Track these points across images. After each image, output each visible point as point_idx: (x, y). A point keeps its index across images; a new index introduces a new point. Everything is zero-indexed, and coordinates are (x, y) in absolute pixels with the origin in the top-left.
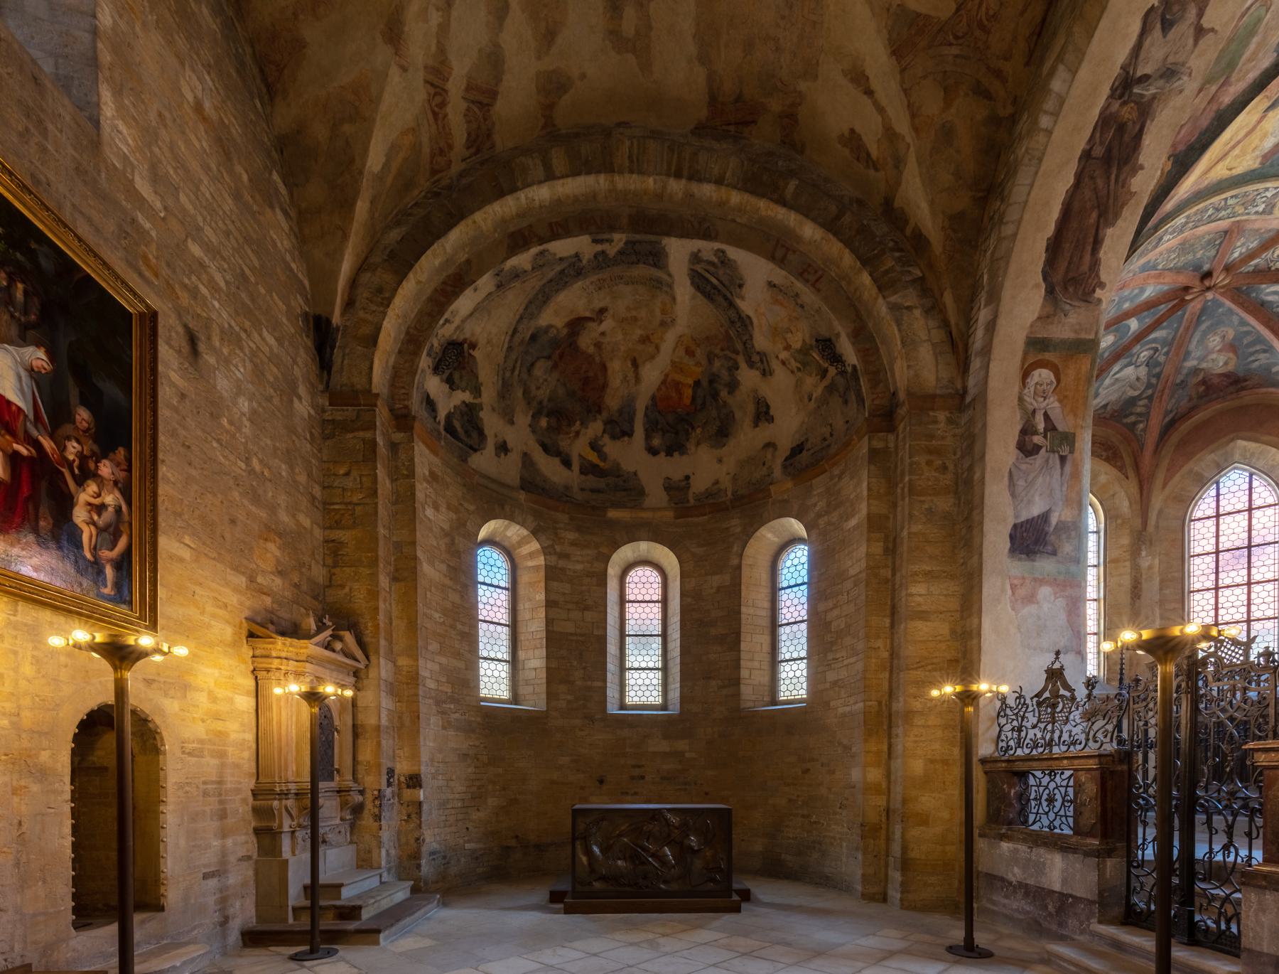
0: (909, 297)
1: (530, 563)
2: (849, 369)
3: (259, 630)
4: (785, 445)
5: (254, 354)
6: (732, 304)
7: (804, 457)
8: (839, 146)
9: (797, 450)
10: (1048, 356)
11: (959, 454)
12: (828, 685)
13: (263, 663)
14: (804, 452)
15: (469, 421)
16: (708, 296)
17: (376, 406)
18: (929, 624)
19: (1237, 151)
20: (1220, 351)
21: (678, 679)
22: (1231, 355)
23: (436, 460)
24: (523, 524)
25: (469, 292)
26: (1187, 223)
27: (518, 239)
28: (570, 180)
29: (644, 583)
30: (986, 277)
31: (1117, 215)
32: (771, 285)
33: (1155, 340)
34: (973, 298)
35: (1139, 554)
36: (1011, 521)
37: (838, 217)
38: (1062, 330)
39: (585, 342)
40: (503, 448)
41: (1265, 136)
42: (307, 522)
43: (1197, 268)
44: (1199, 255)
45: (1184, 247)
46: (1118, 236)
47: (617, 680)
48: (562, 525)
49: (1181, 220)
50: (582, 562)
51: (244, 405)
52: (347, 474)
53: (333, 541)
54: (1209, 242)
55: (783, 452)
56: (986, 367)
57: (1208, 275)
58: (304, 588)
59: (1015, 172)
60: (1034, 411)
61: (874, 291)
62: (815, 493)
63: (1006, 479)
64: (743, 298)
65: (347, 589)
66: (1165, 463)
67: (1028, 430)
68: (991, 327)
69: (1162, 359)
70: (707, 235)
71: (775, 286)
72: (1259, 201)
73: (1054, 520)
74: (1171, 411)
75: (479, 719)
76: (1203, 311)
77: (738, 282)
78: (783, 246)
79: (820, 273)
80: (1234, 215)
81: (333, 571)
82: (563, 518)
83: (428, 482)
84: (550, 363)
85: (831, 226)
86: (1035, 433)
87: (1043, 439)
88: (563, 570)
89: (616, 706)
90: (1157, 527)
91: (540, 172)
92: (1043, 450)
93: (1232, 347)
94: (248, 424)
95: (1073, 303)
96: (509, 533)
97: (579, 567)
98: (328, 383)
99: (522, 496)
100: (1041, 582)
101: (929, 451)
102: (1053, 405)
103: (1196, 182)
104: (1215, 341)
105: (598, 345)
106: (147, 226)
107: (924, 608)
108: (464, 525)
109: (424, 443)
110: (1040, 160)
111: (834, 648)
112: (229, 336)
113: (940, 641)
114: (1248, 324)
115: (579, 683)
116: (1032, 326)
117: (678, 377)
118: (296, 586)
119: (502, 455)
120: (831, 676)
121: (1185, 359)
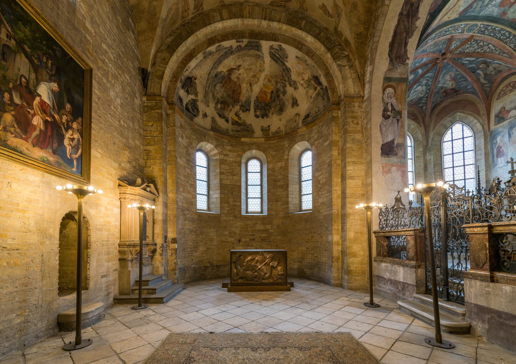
0: (344, 62)
1: (214, 158)
2: (324, 87)
3: (122, 183)
4: (303, 114)
5: (122, 83)
6: (284, 64)
7: (310, 119)
8: (319, 9)
9: (307, 116)
10: (392, 83)
11: (363, 118)
12: (319, 204)
13: (123, 196)
14: (310, 117)
15: (194, 106)
16: (276, 61)
17: (162, 100)
18: (354, 181)
19: (451, 12)
20: (450, 81)
21: (267, 202)
22: (454, 82)
23: (183, 120)
24: (212, 144)
25: (194, 59)
26: (436, 36)
27: (211, 41)
28: (229, 20)
29: (254, 166)
30: (369, 55)
31: (412, 34)
32: (297, 57)
33: (427, 77)
34: (365, 63)
35: (426, 154)
36: (381, 143)
37: (319, 34)
38: (396, 75)
39: (234, 77)
40: (205, 115)
41: (459, 7)
42: (138, 143)
43: (440, 51)
44: (441, 47)
45: (435, 45)
46: (413, 41)
47: (245, 202)
48: (225, 144)
49: (434, 35)
50: (233, 158)
51: (119, 101)
52: (152, 126)
53: (147, 150)
54: (443, 43)
55: (302, 117)
56: (371, 88)
57: (444, 54)
58: (137, 168)
59: (378, 19)
60: (387, 103)
61: (332, 59)
62: (314, 132)
63: (379, 128)
64: (287, 62)
65: (151, 168)
66: (433, 121)
67: (385, 110)
68: (372, 73)
69: (430, 83)
70: (275, 40)
71: (298, 58)
72: (459, 29)
73: (396, 143)
74: (434, 102)
75: (196, 217)
76: (444, 66)
77: (286, 56)
78: (301, 44)
79: (314, 53)
80: (451, 33)
81: (147, 161)
82: (226, 141)
83: (180, 128)
84: (222, 85)
85: (317, 37)
86: (388, 111)
87: (391, 113)
88: (226, 160)
89: (245, 212)
90: (432, 144)
91: (219, 18)
92: (391, 117)
93: (454, 79)
94: (119, 108)
95: (399, 65)
96: (207, 147)
97: (231, 159)
98: (146, 92)
99: (212, 133)
100: (393, 165)
101: (352, 117)
102: (394, 101)
103: (438, 23)
104: (448, 77)
105: (238, 78)
106: (89, 38)
107: (352, 175)
108: (192, 144)
109: (179, 114)
110: (386, 15)
111: (322, 190)
112: (115, 77)
113: (358, 187)
114: (459, 71)
115: (231, 203)
116: (385, 73)
117: (266, 90)
118: (134, 167)
119: (205, 118)
120: (321, 201)
121: (438, 84)
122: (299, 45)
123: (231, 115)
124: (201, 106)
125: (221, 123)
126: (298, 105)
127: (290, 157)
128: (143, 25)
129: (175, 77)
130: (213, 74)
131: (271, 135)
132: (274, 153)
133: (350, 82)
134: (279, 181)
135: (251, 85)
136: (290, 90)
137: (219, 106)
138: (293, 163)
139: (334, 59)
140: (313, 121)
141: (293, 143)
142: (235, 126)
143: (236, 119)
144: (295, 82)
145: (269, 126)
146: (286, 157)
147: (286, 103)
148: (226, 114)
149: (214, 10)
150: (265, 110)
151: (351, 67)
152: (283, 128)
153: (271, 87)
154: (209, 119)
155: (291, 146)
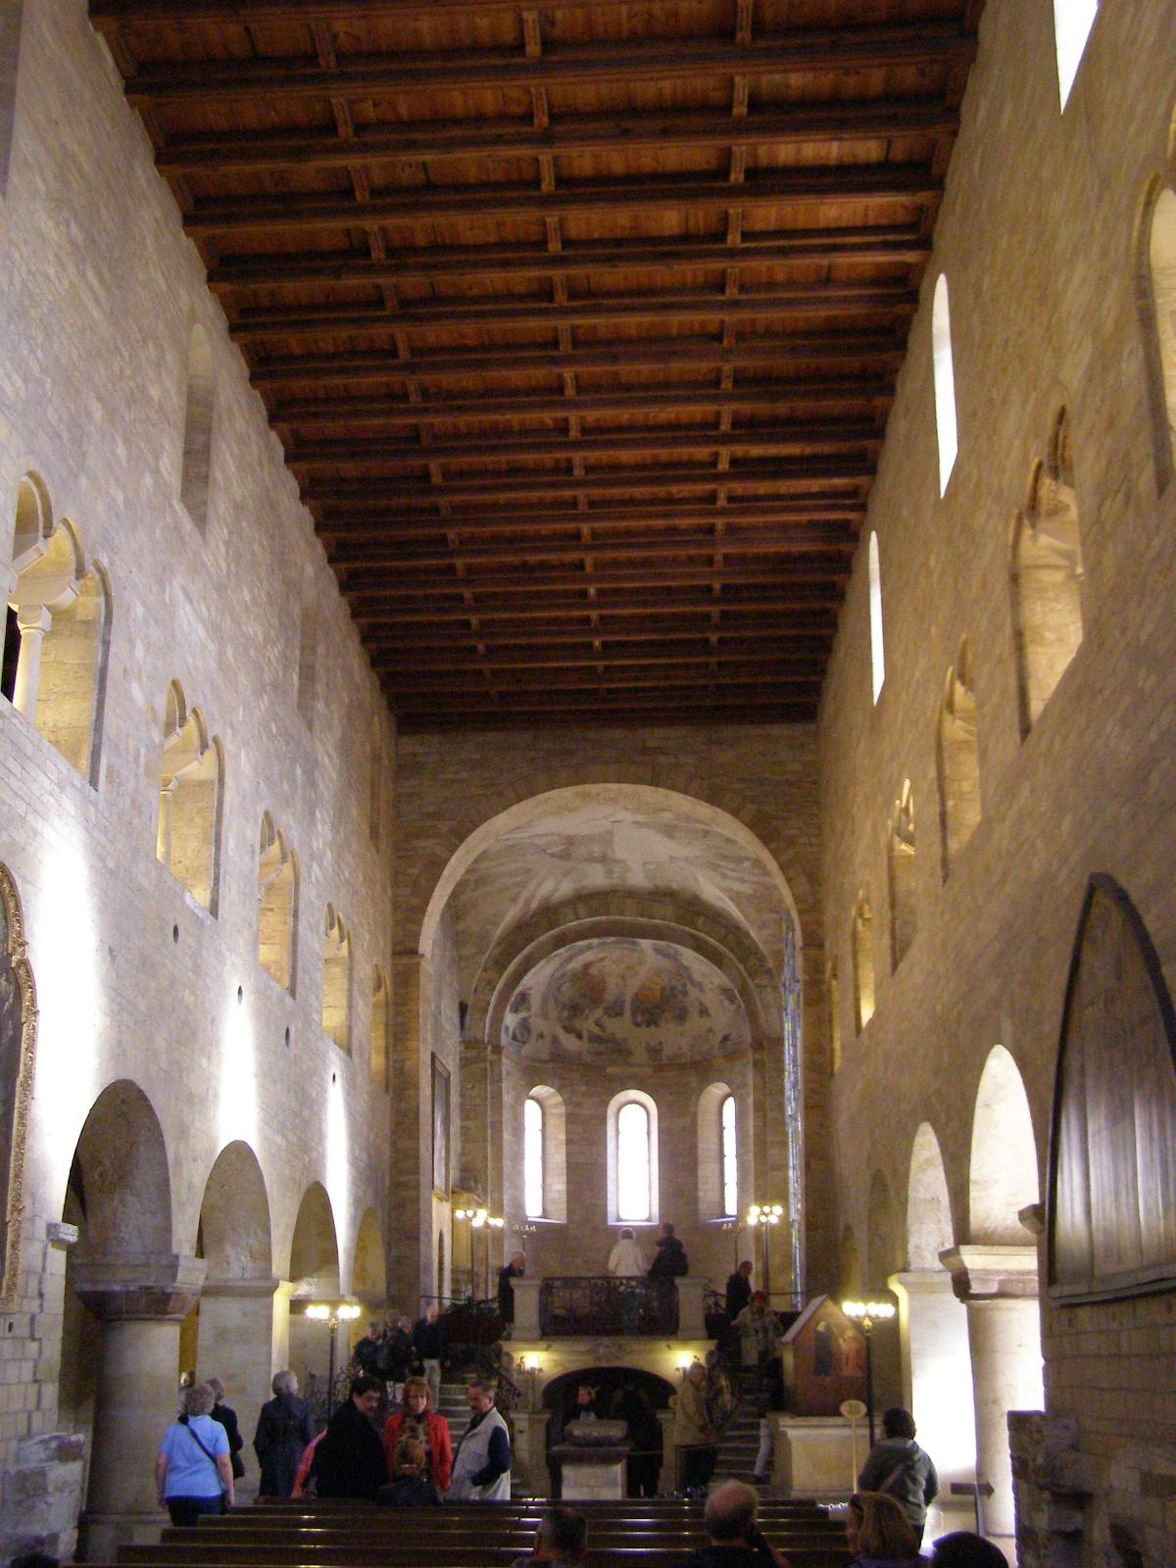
9: (726, 1038)
55: (719, 1037)
122: (701, 947)
123: (587, 1025)
124: (537, 1024)
125: (570, 1043)
126: (709, 1015)
127: (700, 1109)
128: (469, 950)
129: (503, 999)
130: (557, 975)
131: (664, 1061)
135: (623, 978)
136: (693, 993)
137: (565, 1014)
138: (705, 1119)
139: (750, 975)
141: (705, 1082)
143: (597, 1030)
144: (700, 984)
145: (661, 1043)
148: (578, 1023)
150: (652, 1014)
152: (685, 1049)
154: (548, 1040)
155: (701, 1089)
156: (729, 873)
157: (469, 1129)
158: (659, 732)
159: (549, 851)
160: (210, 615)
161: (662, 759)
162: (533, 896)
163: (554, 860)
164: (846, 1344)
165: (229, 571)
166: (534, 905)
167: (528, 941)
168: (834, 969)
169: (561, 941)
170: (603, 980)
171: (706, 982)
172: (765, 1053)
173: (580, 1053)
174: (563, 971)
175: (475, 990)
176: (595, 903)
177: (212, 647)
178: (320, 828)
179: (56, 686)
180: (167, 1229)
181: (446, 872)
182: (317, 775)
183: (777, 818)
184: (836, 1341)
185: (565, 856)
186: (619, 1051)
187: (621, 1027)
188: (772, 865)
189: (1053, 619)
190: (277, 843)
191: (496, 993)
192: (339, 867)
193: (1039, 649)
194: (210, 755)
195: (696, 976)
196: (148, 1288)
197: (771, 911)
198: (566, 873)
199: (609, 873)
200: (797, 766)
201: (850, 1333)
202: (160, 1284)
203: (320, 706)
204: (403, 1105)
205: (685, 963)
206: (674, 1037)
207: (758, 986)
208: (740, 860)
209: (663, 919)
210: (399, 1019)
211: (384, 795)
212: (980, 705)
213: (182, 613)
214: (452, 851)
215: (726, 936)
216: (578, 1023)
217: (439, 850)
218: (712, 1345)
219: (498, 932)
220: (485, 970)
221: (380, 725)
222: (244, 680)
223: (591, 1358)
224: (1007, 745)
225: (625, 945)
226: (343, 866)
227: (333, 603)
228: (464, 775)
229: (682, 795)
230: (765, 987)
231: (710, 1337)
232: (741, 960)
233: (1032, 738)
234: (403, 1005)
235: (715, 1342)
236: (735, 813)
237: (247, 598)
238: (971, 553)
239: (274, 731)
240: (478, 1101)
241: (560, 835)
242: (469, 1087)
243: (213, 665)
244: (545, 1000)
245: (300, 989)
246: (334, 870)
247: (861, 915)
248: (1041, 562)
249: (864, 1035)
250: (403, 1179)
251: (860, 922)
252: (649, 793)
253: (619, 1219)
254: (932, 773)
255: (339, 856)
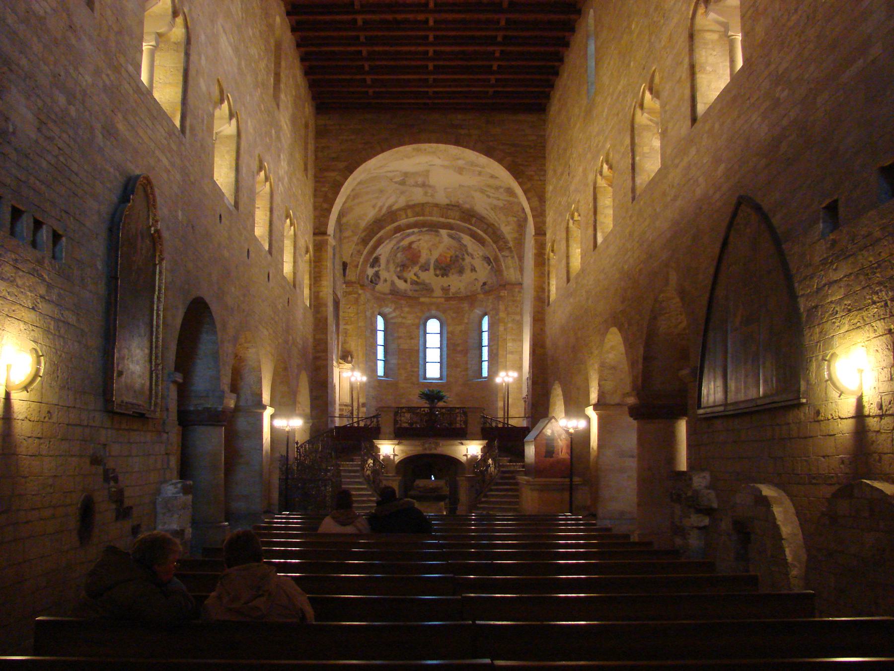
7: (487, 287)
9: (485, 284)
29: (433, 325)
99: (390, 297)
117: (445, 255)
123: (410, 275)
124: (384, 274)
125: (401, 285)
126: (476, 271)
129: (366, 260)
130: (396, 248)
131: (451, 295)
132: (454, 315)
133: (512, 270)
134: (458, 345)
135: (430, 251)
136: (468, 259)
137: (399, 269)
139: (499, 250)
140: (490, 291)
141: (472, 305)
142: (414, 286)
143: (415, 278)
145: (449, 286)
146: (466, 321)
147: (466, 268)
148: (405, 274)
149: (400, 209)
150: (445, 270)
151: (513, 257)
152: (462, 290)
153: (452, 253)
154: (389, 283)
156: (491, 195)
157: (348, 330)
158: (460, 117)
159: (393, 180)
160: (234, 42)
161: (462, 132)
162: (384, 205)
163: (397, 185)
164: (562, 443)
165: (242, 18)
166: (384, 210)
167: (381, 228)
168: (553, 246)
169: (398, 230)
170: (420, 251)
171: (475, 253)
172: (506, 292)
173: (406, 290)
174: (398, 246)
175: (352, 254)
176: (417, 209)
177: (236, 61)
178: (282, 163)
179: (160, 79)
180: (218, 378)
181: (342, 190)
182: (281, 135)
183: (523, 165)
184: (557, 440)
185: (403, 183)
186: (427, 290)
187: (428, 277)
188: (519, 191)
189: (711, 60)
190: (263, 172)
191: (363, 257)
192: (291, 185)
193: (703, 76)
194: (234, 121)
195: (470, 250)
196: (208, 409)
197: (513, 216)
198: (402, 193)
199: (426, 194)
200: (534, 138)
201: (564, 436)
202: (215, 406)
203: (283, 96)
204: (318, 316)
205: (465, 242)
206: (457, 283)
207: (503, 256)
208: (497, 188)
209: (454, 219)
210: (317, 270)
211: (311, 147)
212: (663, 106)
213: (222, 40)
214: (346, 179)
215: (487, 229)
216: (405, 274)
217: (338, 178)
218: (485, 442)
219: (363, 224)
220: (357, 244)
221: (308, 109)
222: (249, 79)
223: (421, 449)
224: (683, 127)
225: (430, 233)
226: (292, 185)
227: (288, 39)
228: (353, 137)
229: (471, 151)
230: (507, 257)
231: (483, 439)
232: (495, 242)
233: (698, 125)
234: (318, 262)
235: (485, 442)
236: (500, 161)
237: (251, 34)
238: (662, 21)
239: (263, 109)
240: (352, 315)
241: (401, 172)
242: (348, 307)
243: (236, 70)
244: (388, 262)
245: (274, 251)
246: (288, 187)
247: (572, 218)
248: (706, 28)
249: (572, 283)
250: (319, 355)
251: (571, 221)
252: (453, 150)
253: (425, 378)
254: (628, 141)
255: (290, 179)
